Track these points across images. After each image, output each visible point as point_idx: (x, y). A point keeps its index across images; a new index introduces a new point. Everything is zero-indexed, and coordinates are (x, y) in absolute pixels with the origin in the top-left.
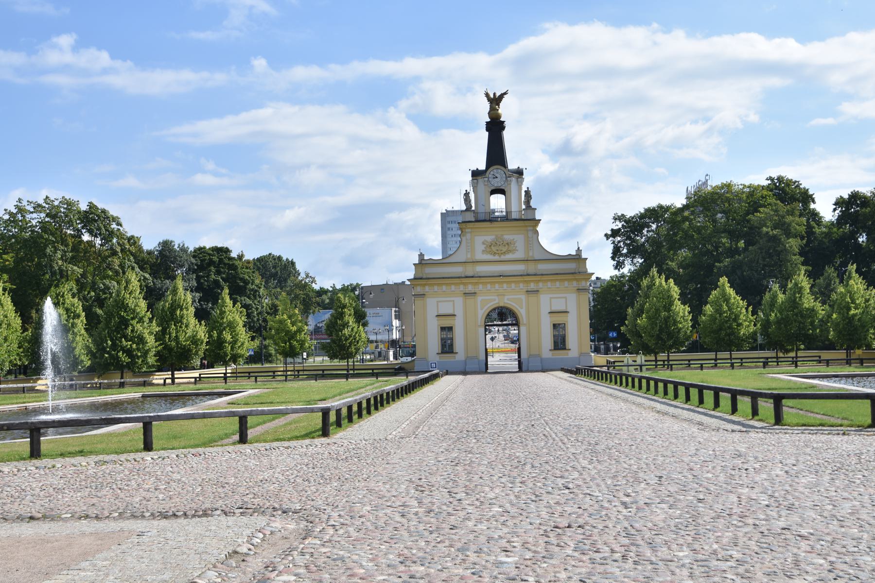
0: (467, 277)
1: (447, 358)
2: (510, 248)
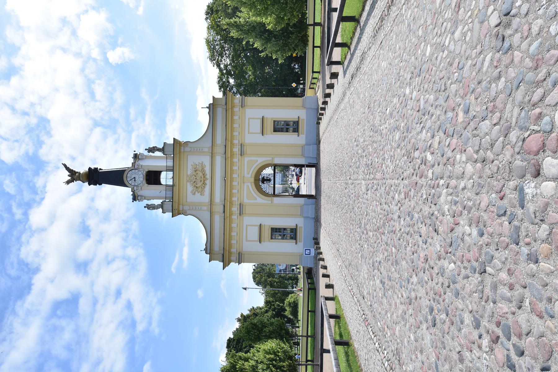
0: (224, 212)
1: (301, 234)
2: (200, 169)
